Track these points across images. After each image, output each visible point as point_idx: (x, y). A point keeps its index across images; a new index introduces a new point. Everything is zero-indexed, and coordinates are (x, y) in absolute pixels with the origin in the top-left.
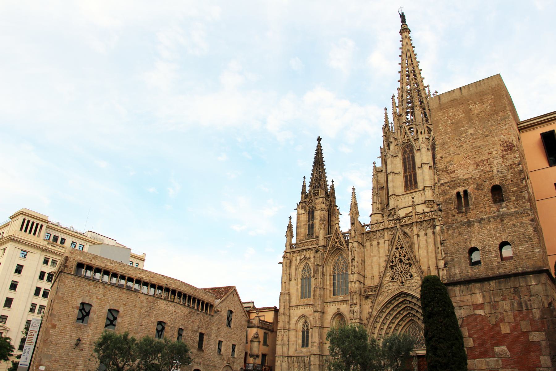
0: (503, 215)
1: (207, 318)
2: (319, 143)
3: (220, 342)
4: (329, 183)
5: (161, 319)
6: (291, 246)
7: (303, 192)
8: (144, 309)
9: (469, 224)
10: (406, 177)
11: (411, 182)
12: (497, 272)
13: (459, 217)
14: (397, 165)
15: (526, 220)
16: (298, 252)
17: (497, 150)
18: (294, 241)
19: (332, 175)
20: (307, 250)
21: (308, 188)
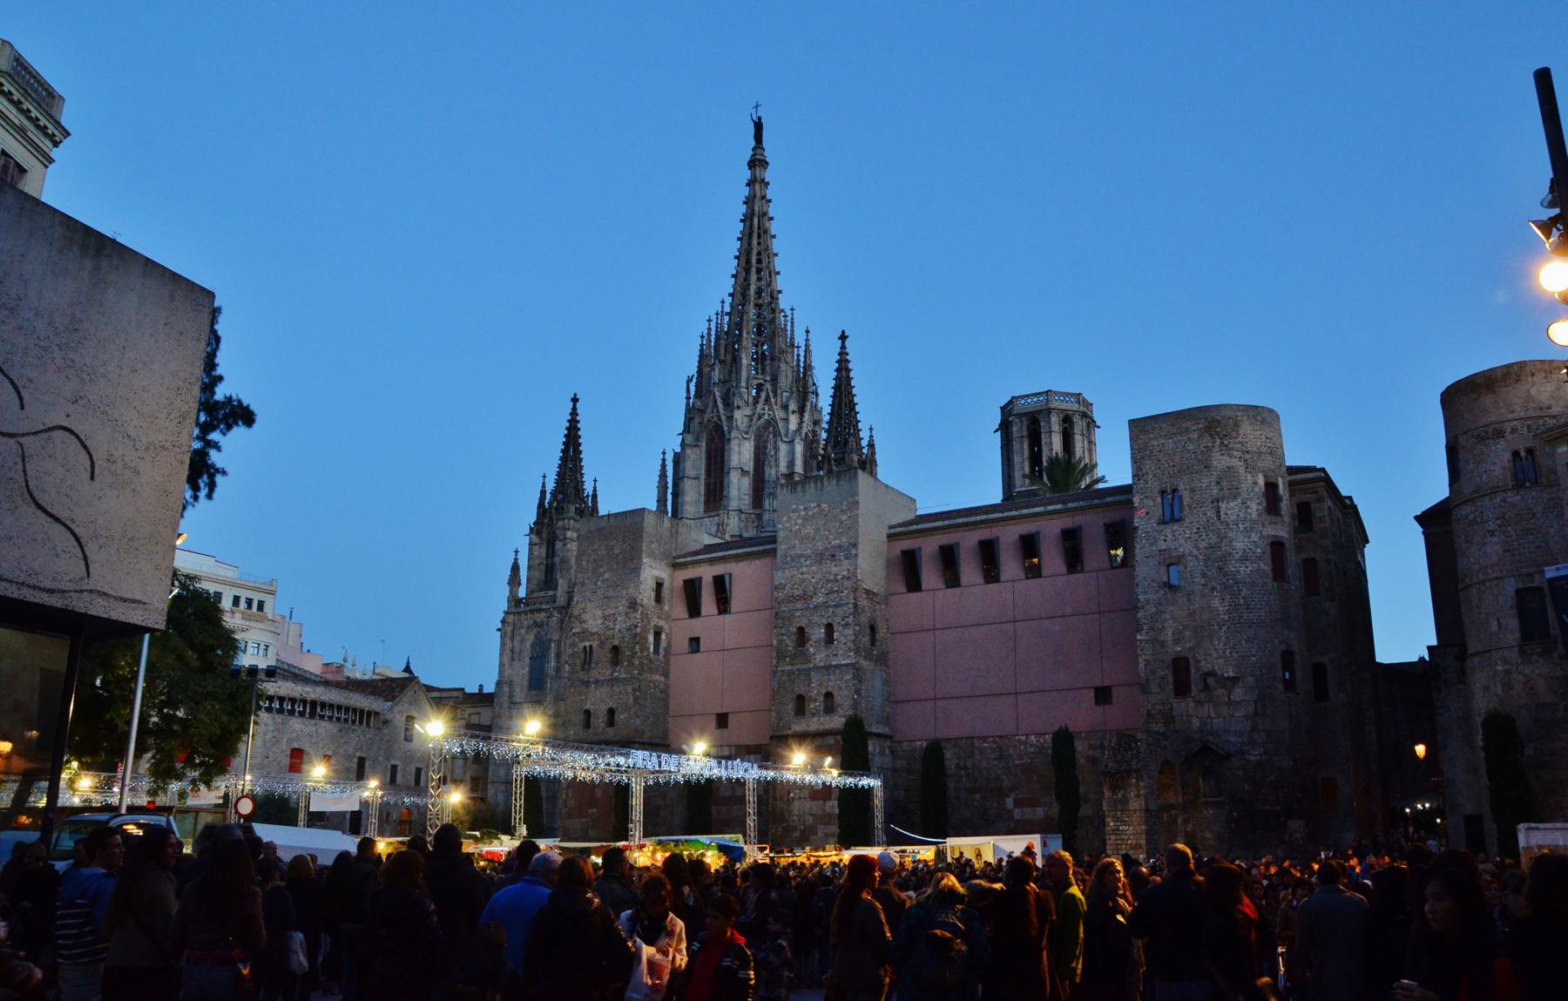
0: (616, 679)
1: (370, 733)
2: (574, 408)
3: (394, 768)
4: (588, 488)
5: (296, 745)
6: (514, 601)
7: (541, 505)
8: (269, 736)
9: (587, 684)
10: (707, 485)
11: (715, 496)
12: (602, 738)
13: (581, 675)
14: (696, 463)
15: (630, 689)
16: (525, 613)
17: (622, 606)
18: (522, 593)
19: (592, 470)
20: (539, 611)
21: (548, 496)
